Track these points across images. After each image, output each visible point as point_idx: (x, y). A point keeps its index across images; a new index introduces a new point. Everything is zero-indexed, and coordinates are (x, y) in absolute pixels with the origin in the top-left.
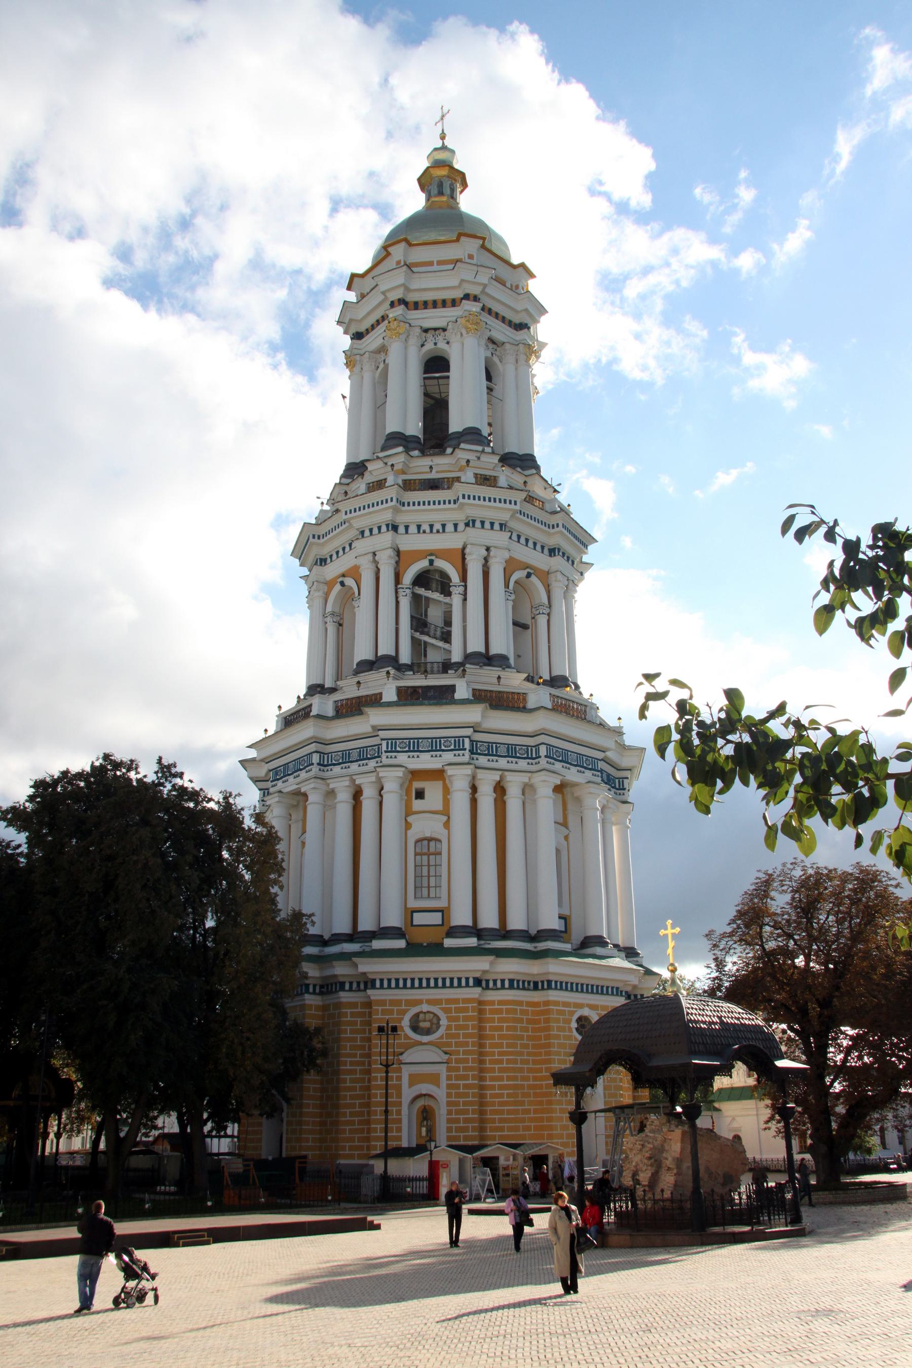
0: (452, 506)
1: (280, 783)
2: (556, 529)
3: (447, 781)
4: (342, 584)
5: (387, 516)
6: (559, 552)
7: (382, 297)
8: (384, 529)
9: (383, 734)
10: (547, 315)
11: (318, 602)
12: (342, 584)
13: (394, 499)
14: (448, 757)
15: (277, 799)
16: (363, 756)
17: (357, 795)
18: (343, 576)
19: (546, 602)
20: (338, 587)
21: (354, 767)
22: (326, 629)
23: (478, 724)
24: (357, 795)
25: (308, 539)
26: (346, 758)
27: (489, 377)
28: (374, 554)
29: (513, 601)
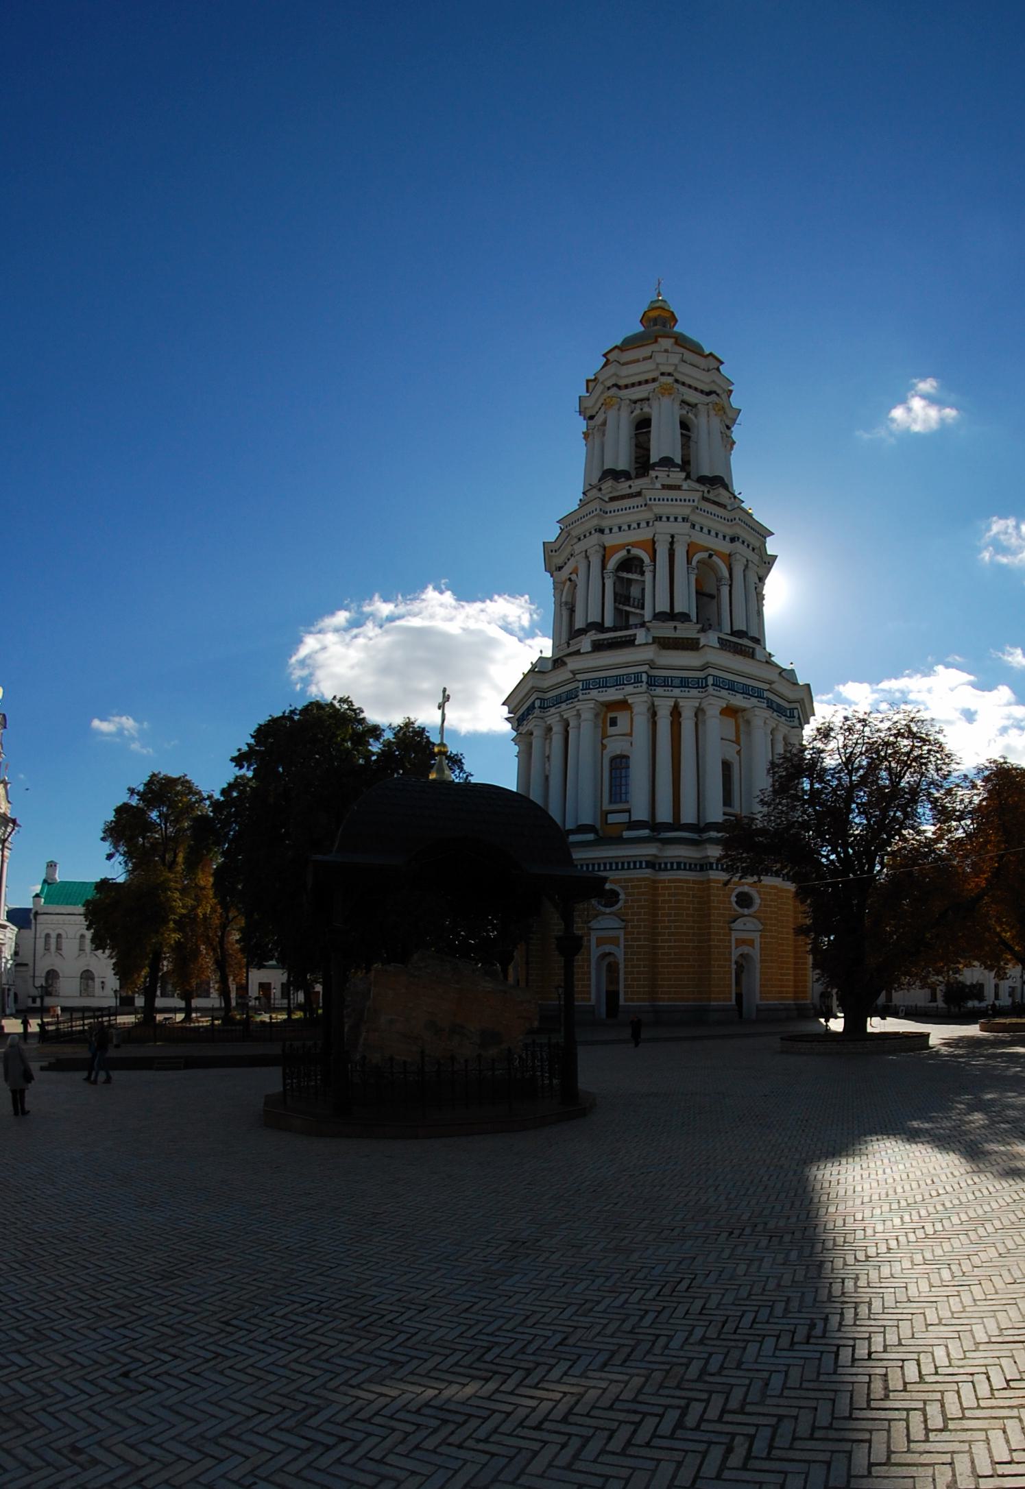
1: (594, 693)
3: (741, 720)
4: (629, 551)
5: (687, 511)
8: (680, 519)
9: (711, 671)
12: (629, 551)
14: (754, 700)
15: (592, 706)
16: (684, 683)
17: (676, 712)
20: (623, 553)
21: (677, 692)
24: (676, 712)
26: (666, 683)
28: (673, 537)
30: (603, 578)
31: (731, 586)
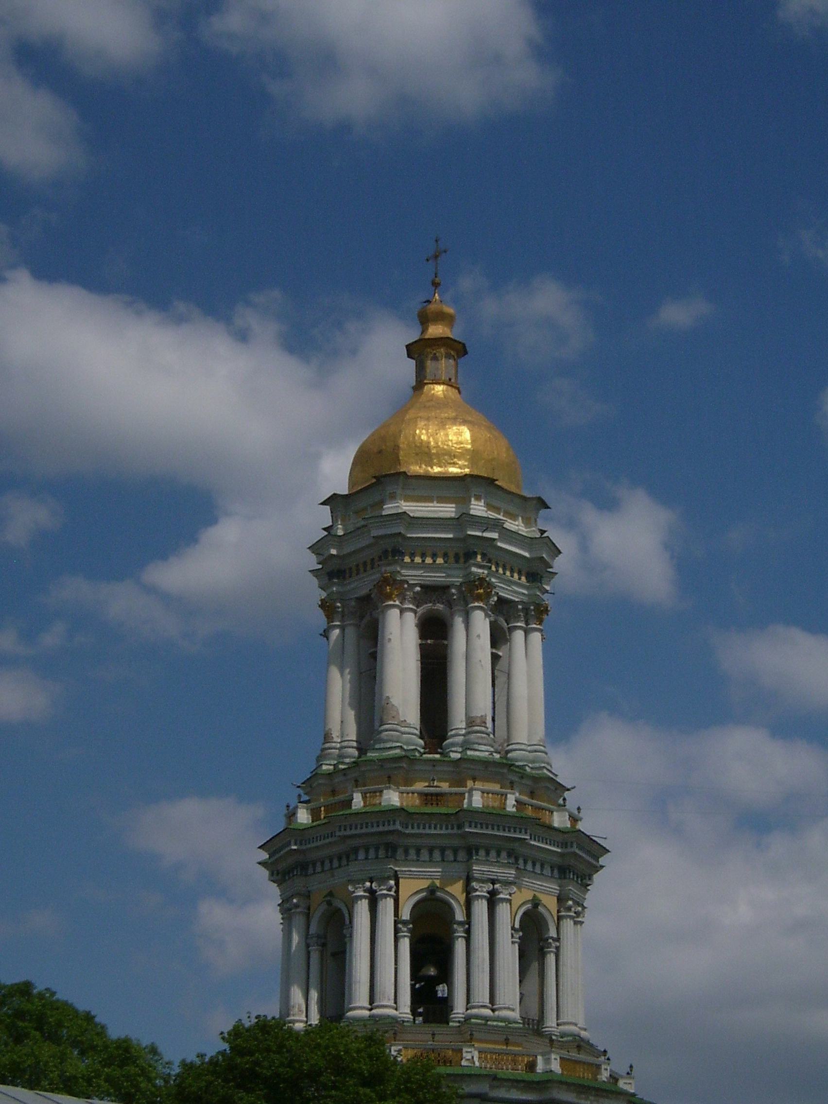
0: (455, 831)
2: (569, 850)
4: (329, 903)
6: (570, 872)
7: (372, 541)
10: (561, 554)
11: (299, 921)
12: (329, 903)
13: (398, 823)
18: (331, 894)
19: (555, 936)
20: (324, 906)
22: (308, 953)
23: (486, 1094)
25: (289, 844)
27: (494, 643)
29: (520, 938)
30: (308, 946)
31: (468, 932)
